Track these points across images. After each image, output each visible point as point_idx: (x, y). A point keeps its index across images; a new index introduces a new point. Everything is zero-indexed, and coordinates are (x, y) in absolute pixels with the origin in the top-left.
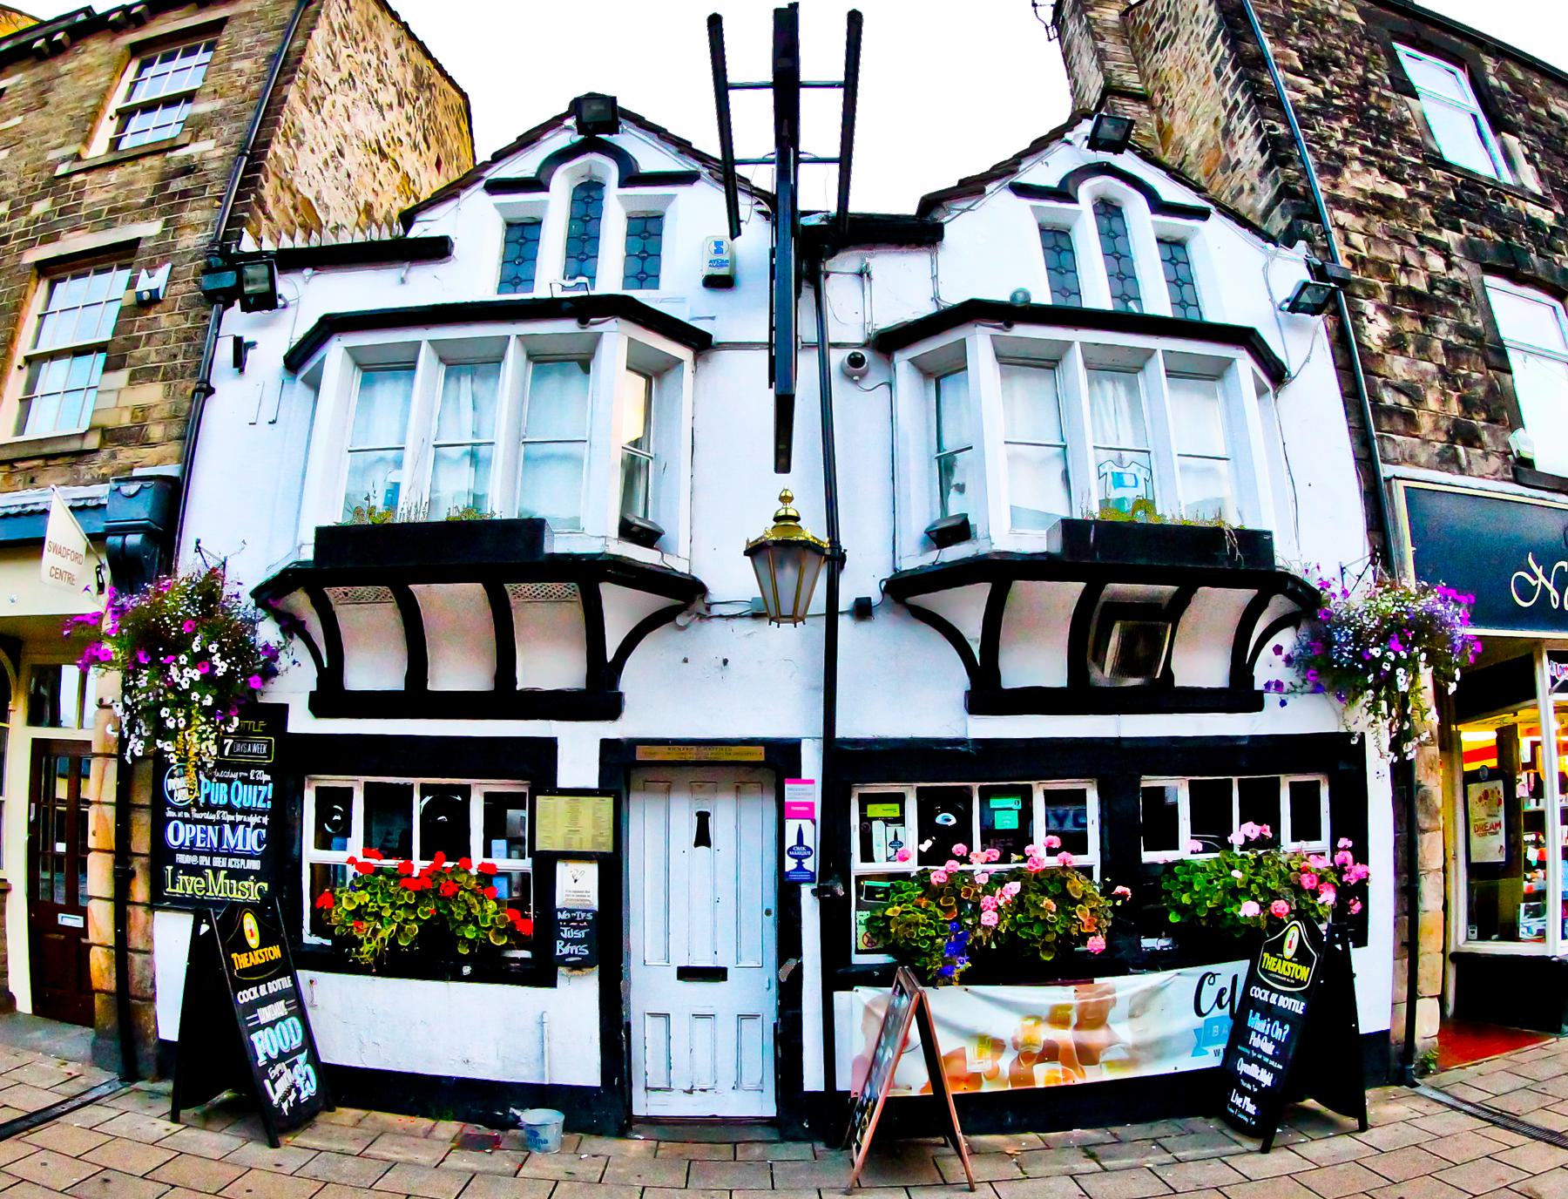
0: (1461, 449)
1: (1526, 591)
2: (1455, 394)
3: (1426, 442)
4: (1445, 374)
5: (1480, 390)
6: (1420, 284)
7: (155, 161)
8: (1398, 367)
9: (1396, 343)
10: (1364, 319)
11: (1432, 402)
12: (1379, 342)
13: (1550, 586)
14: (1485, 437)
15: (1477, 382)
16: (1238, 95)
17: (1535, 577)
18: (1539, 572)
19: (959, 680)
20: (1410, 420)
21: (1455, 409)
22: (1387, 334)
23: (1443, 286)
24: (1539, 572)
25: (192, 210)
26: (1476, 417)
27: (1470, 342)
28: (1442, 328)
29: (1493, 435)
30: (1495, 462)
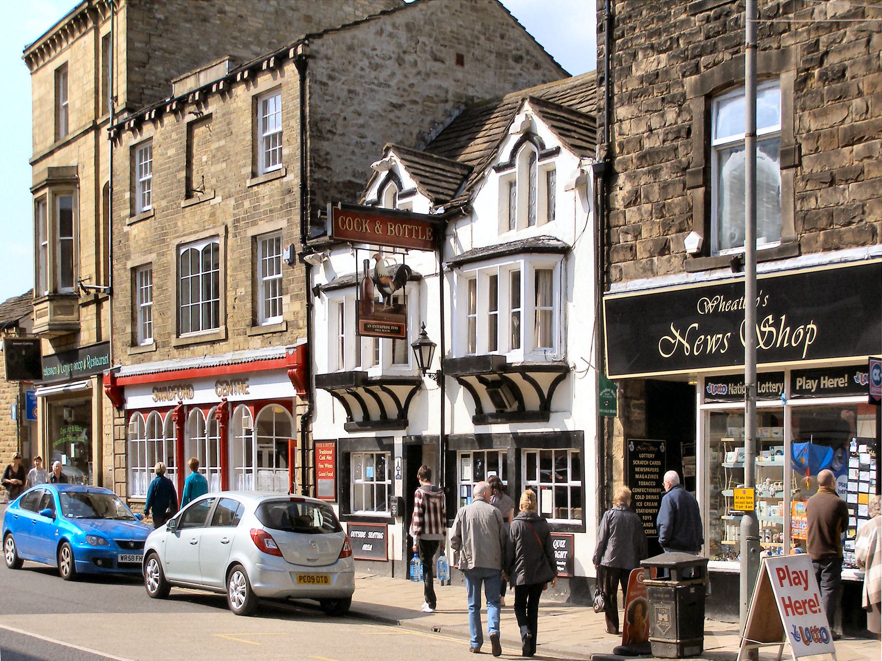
0: (655, 259)
1: (667, 347)
5: (677, 211)
7: (277, 182)
8: (632, 215)
10: (618, 189)
11: (644, 234)
13: (684, 342)
14: (672, 246)
15: (677, 205)
17: (674, 338)
18: (677, 335)
22: (627, 195)
24: (677, 335)
27: (679, 175)
28: (663, 173)
30: (676, 261)
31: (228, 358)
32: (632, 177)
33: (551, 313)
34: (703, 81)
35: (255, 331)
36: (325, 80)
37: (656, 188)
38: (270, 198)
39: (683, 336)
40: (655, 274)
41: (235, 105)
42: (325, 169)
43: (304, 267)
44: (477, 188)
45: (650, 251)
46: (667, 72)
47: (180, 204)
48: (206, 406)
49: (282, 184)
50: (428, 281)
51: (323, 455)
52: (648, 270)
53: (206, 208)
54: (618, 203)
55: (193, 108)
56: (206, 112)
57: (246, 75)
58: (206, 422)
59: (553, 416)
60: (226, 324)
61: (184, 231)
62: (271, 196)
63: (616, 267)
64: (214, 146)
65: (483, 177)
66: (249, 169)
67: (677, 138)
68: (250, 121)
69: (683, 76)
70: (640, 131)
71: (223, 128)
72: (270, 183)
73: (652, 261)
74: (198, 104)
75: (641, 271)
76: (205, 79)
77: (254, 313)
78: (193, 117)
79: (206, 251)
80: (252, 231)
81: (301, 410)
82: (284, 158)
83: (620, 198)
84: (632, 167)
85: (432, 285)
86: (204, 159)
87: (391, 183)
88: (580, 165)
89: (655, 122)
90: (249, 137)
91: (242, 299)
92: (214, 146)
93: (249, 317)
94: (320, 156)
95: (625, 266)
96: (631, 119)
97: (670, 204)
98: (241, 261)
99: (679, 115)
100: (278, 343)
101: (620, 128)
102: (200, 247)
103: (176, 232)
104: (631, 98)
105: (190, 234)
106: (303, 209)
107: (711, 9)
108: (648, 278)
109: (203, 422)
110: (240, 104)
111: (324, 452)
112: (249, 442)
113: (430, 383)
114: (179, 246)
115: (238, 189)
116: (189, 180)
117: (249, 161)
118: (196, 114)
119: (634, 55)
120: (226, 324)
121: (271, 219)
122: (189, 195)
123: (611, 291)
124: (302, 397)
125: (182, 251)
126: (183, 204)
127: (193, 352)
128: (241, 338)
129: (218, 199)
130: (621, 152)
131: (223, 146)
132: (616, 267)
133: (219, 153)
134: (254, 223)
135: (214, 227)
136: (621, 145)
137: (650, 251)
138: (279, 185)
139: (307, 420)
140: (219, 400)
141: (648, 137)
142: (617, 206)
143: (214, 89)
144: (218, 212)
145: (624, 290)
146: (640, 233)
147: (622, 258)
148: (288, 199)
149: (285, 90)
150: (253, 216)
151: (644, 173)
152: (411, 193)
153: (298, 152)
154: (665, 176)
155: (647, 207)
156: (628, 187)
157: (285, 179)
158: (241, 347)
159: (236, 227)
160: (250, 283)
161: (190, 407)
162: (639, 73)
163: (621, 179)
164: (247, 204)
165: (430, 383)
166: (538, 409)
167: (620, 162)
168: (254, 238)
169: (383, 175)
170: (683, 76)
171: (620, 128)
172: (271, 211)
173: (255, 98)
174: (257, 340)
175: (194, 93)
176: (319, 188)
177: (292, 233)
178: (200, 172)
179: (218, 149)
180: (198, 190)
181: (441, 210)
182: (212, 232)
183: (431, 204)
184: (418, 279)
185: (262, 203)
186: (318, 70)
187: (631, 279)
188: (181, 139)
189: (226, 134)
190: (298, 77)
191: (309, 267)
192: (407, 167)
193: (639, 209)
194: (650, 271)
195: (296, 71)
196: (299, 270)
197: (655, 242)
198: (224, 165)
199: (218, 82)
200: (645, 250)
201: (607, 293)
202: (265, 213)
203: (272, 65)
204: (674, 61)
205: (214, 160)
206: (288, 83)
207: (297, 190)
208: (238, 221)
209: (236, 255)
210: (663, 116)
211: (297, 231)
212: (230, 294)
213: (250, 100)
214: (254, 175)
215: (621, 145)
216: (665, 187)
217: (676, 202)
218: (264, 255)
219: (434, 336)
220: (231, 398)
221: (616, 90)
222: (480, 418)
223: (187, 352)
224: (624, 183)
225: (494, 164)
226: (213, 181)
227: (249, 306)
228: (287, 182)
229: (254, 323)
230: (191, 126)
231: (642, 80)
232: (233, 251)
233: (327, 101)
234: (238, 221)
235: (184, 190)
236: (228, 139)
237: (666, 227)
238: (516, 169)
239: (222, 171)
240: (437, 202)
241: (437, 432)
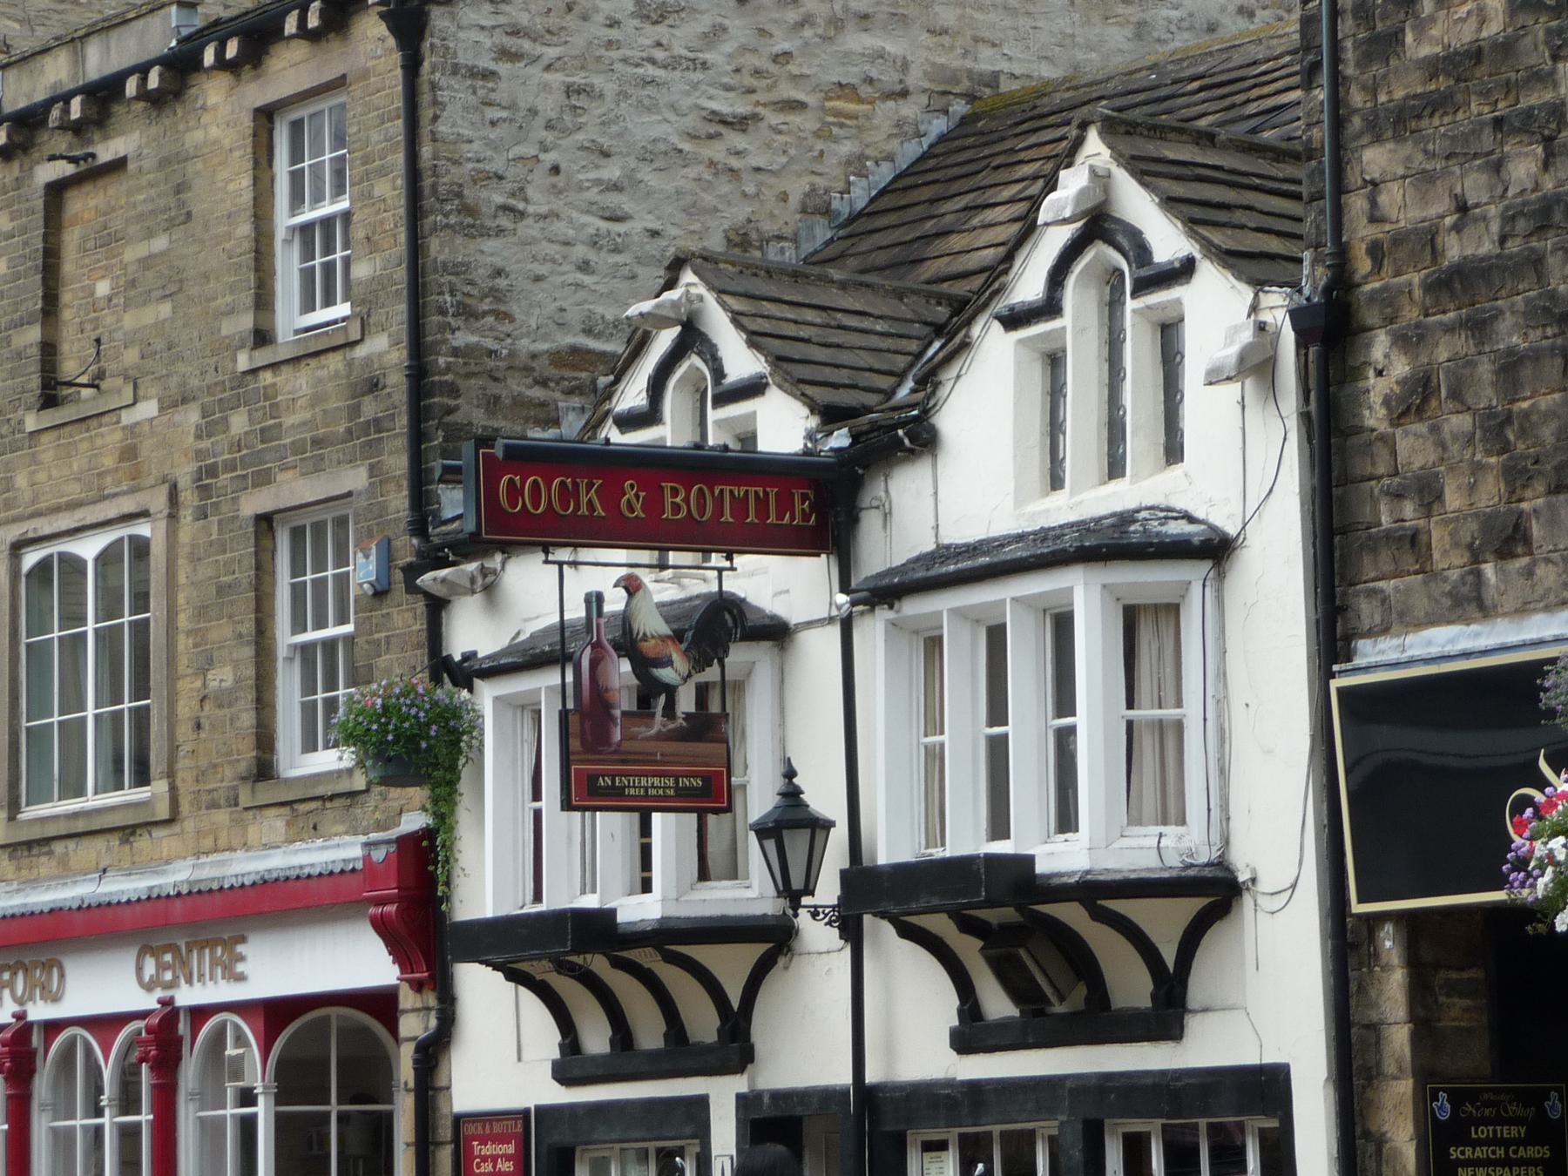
0: (1489, 569)
5: (1547, 433)
7: (334, 362)
10: (1371, 373)
11: (1453, 500)
12: (1382, 412)
14: (1536, 531)
20: (1414, 542)
21: (1490, 493)
22: (1397, 389)
25: (390, 453)
26: (1528, 493)
27: (1549, 331)
28: (1505, 324)
31: (177, 875)
32: (1408, 341)
33: (1179, 726)
35: (266, 793)
36: (485, 62)
37: (1485, 370)
38: (313, 406)
41: (198, 135)
42: (490, 319)
43: (421, 606)
44: (948, 375)
45: (1470, 547)
46: (1505, 48)
47: (21, 422)
48: (104, 1025)
49: (350, 364)
51: (484, 1159)
52: (1469, 600)
53: (111, 437)
54: (1375, 417)
55: (61, 143)
56: (106, 152)
57: (232, 50)
58: (107, 1074)
59: (1193, 1024)
60: (171, 775)
61: (33, 502)
62: (317, 399)
63: (1372, 593)
64: (133, 253)
65: (965, 345)
66: (246, 322)
67: (1541, 229)
68: (246, 181)
69: (1555, 58)
70: (1433, 211)
71: (162, 202)
72: (313, 362)
73: (1478, 574)
74: (78, 129)
75: (1447, 602)
76: (98, 61)
77: (265, 740)
78: (67, 169)
79: (107, 558)
80: (255, 503)
81: (414, 1026)
82: (355, 290)
83: (1376, 398)
84: (1410, 314)
85: (820, 649)
86: (103, 288)
87: (694, 361)
88: (1254, 308)
90: (245, 229)
91: (223, 699)
92: (133, 253)
93: (247, 754)
94: (471, 283)
95: (1396, 589)
96: (1404, 177)
97: (1526, 414)
98: (221, 590)
99: (1546, 166)
100: (340, 828)
101: (1373, 203)
102: (88, 548)
103: (8, 505)
105: (57, 509)
106: (417, 437)
108: (1467, 621)
109: (94, 1072)
110: (214, 132)
111: (489, 1149)
112: (247, 1127)
113: (818, 935)
114: (17, 548)
115: (211, 378)
116: (49, 350)
117: (247, 298)
118: (73, 160)
120: (171, 775)
121: (317, 466)
122: (49, 400)
123: (1359, 661)
124: (418, 986)
125: (31, 559)
126: (31, 422)
127: (64, 862)
128: (222, 816)
129: (148, 409)
130: (1378, 265)
131: (162, 254)
132: (1372, 593)
133: (150, 274)
134: (264, 480)
135: (133, 491)
136: (1376, 251)
137: (1470, 547)
138: (340, 366)
139: (434, 1050)
140: (149, 1002)
141: (1457, 228)
142: (1370, 422)
143: (131, 87)
144: (146, 448)
145: (1393, 656)
146: (1439, 497)
147: (1387, 567)
148: (370, 408)
149: (358, 94)
150: (258, 457)
151: (1449, 329)
152: (752, 389)
153: (401, 274)
154: (1511, 335)
155: (1460, 422)
156: (1401, 367)
157: (360, 352)
158: (222, 842)
159: (204, 491)
160: (248, 652)
161: (53, 1027)
162: (1426, 51)
163: (1380, 346)
164: (239, 422)
165: (818, 935)
166: (1149, 1005)
167: (1373, 297)
168: (265, 522)
169: (665, 340)
170: (1555, 58)
171: (1373, 203)
172: (317, 442)
173: (266, 116)
174: (275, 823)
175: (66, 98)
176: (469, 375)
177: (383, 508)
178: (88, 326)
179: (146, 263)
180: (84, 379)
181: (840, 439)
182: (128, 505)
183: (814, 422)
184: (777, 633)
185: (289, 420)
186: (462, 35)
188: (24, 230)
189: (171, 219)
190: (397, 57)
191: (437, 607)
192: (737, 319)
193: (1435, 429)
195: (391, 42)
196: (406, 618)
197: (1488, 521)
198: (165, 309)
199: (143, 70)
200: (1456, 545)
201: (1344, 666)
202: (298, 448)
203: (313, 22)
205: (132, 293)
206: (365, 74)
207: (397, 382)
208: (212, 471)
209: (205, 572)
210: (1497, 167)
211: (399, 501)
212: (188, 686)
213: (247, 122)
214: (262, 337)
215: (1376, 251)
216: (1511, 368)
217: (1543, 406)
218: (297, 569)
219: (827, 798)
220: (187, 996)
221: (1357, 98)
223: (45, 865)
224: (1386, 356)
225: (1001, 305)
226: (131, 356)
227: (247, 719)
228: (368, 360)
229: (264, 770)
230: (56, 191)
231: (1433, 67)
232: (195, 559)
233: (493, 123)
234: (212, 471)
235: (35, 382)
236: (178, 233)
237: (1516, 476)
238: (1066, 321)
239: (159, 325)
240: (830, 416)
241: (842, 1076)
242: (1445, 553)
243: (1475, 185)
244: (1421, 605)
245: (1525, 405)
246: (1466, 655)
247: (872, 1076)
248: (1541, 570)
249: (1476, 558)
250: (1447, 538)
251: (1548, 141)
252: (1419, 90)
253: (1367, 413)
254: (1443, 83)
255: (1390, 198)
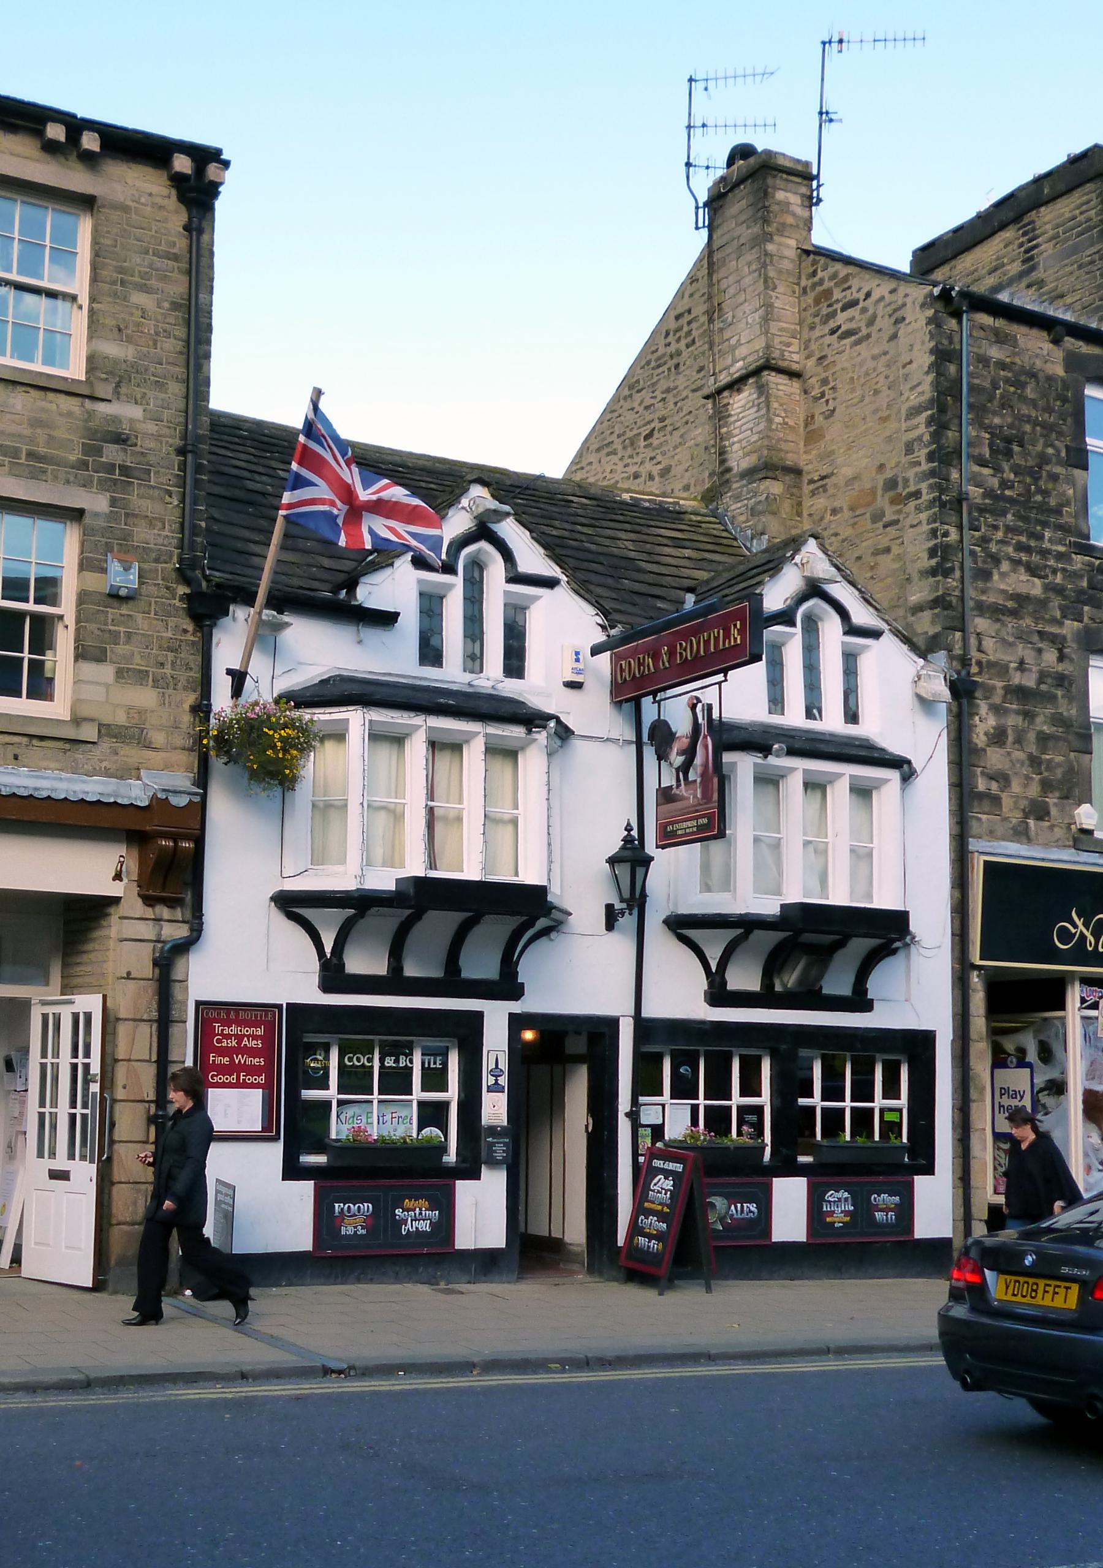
0: (1031, 822)
1: (1065, 936)
2: (1037, 777)
3: (1006, 819)
4: (1034, 762)
5: (1059, 773)
6: (1029, 681)
8: (995, 758)
9: (998, 737)
10: (977, 718)
11: (1016, 787)
12: (984, 738)
14: (1054, 811)
15: (1059, 765)
16: (924, 486)
17: (1075, 926)
18: (1081, 927)
19: (701, 983)
20: (996, 800)
21: (1034, 791)
22: (992, 731)
23: (1049, 681)
24: (1079, 923)
26: (1050, 795)
27: (1061, 730)
28: (1039, 719)
29: (1062, 810)
30: (1059, 832)
32: (996, 709)
34: (1087, 630)
37: (1032, 736)
39: (1087, 927)
40: (1028, 839)
45: (1023, 810)
46: (1043, 603)
50: (576, 744)
69: (1064, 617)
70: (1007, 658)
89: (1022, 651)
104: (996, 612)
107: (1097, 558)
119: (996, 560)
137: (1023, 810)
147: (986, 809)
155: (1019, 755)
156: (992, 721)
162: (1002, 587)
163: (983, 707)
170: (1064, 617)
187: (998, 839)
194: (1021, 834)
197: (1033, 803)
204: (1051, 595)
210: (1040, 651)
216: (1043, 739)
217: (1056, 761)
222: (718, 995)
224: (987, 714)
237: (1046, 786)
242: (1011, 810)
243: (1029, 656)
244: (1000, 830)
245: (1048, 757)
246: (1043, 860)
247: (643, 1015)
248: (1056, 829)
249: (1026, 816)
250: (1012, 804)
251: (1060, 650)
252: (1001, 602)
253: (975, 736)
254: (1010, 604)
255: (989, 644)
